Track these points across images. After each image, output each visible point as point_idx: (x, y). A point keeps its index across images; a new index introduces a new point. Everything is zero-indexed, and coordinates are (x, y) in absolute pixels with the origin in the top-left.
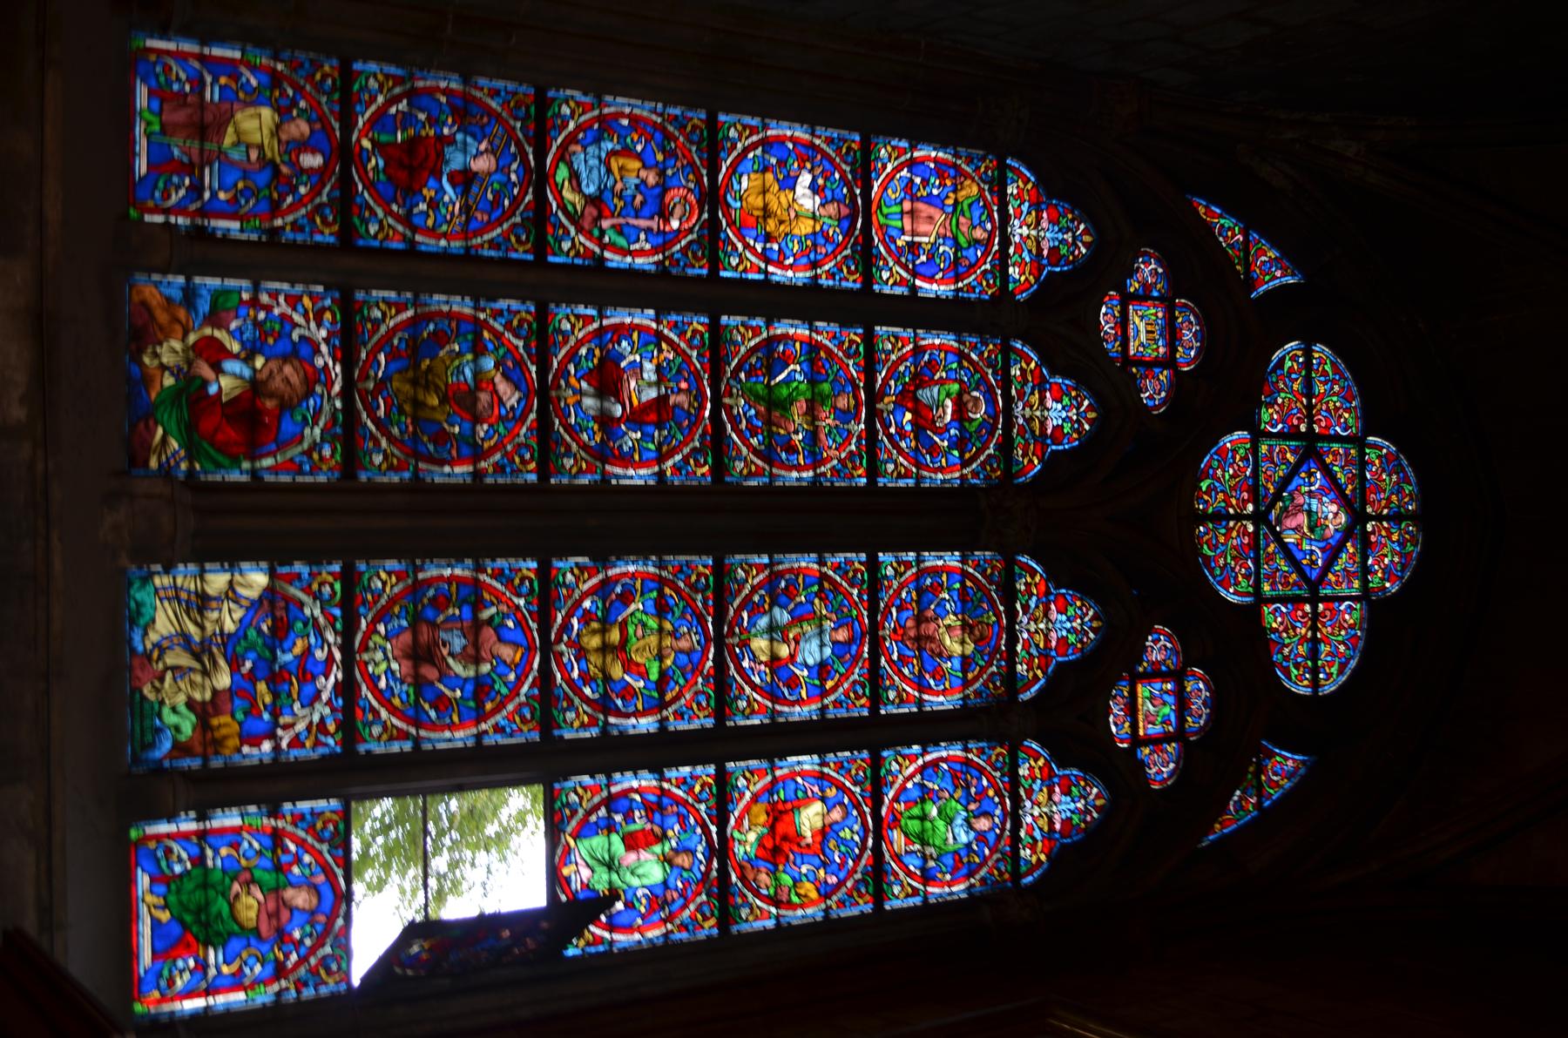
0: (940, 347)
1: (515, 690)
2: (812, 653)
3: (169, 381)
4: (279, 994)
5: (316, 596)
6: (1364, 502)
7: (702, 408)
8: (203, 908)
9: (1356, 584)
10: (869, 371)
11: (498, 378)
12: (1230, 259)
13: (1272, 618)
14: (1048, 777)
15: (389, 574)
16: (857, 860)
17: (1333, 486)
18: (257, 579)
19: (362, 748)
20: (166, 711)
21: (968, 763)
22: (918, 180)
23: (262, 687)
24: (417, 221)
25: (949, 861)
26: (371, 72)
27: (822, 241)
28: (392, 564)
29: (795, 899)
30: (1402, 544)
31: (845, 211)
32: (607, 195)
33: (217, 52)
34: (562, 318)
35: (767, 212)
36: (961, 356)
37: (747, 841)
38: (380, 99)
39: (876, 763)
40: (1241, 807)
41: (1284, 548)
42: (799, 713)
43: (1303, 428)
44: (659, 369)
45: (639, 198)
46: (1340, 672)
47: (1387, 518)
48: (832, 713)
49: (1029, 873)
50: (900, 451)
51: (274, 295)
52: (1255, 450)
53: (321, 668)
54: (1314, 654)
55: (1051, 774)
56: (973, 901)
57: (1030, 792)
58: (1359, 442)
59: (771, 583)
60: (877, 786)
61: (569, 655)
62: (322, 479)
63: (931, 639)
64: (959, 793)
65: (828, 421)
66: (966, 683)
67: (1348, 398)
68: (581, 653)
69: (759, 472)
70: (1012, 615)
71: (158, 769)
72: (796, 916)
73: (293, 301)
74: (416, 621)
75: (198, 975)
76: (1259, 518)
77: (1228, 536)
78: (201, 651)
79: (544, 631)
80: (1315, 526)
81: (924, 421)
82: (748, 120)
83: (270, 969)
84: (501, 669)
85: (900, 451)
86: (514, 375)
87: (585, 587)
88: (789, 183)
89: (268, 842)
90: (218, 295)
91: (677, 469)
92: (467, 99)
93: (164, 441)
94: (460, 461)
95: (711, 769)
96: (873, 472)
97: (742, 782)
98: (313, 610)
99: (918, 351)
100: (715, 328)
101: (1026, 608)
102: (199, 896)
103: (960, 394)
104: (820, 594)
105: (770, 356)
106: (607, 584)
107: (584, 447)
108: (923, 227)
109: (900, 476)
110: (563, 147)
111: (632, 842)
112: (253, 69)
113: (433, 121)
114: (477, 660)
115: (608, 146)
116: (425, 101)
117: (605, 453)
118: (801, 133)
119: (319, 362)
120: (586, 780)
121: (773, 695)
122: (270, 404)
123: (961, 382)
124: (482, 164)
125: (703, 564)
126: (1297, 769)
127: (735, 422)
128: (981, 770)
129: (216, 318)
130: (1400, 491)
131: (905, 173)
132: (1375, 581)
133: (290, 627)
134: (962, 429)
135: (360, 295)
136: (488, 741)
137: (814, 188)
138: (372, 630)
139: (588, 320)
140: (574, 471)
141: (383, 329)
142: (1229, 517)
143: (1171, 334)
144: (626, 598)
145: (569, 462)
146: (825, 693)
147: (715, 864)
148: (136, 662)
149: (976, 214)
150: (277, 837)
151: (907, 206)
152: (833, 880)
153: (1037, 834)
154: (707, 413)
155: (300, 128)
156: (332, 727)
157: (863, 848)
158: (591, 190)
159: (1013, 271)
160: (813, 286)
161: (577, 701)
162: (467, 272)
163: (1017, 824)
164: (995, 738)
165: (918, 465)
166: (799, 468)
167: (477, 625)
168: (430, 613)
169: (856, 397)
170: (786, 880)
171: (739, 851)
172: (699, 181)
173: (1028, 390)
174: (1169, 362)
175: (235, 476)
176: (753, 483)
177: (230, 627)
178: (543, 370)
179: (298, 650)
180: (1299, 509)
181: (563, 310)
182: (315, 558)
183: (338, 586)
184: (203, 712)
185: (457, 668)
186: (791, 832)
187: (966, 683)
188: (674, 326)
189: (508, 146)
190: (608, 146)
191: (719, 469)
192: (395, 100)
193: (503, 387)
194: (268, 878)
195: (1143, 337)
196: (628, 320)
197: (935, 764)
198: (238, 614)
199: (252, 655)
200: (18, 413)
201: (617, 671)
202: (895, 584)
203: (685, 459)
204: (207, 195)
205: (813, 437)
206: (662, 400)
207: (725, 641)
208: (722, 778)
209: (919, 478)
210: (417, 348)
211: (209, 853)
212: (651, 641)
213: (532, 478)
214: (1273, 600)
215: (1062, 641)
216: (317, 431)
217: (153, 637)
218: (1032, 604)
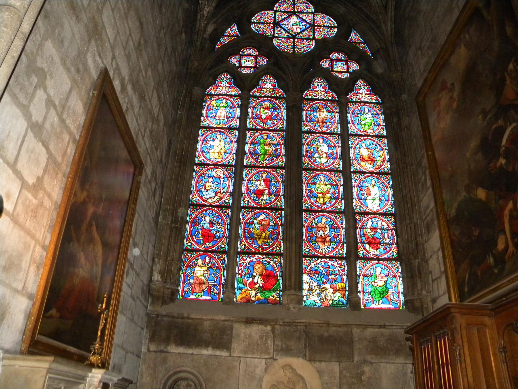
1: (333, 219)
2: (324, 148)
3: (259, 294)
4: (399, 277)
6: (290, 12)
7: (266, 171)
9: (310, 15)
10: (258, 130)
11: (259, 219)
12: (230, 41)
13: (319, 37)
14: (356, 94)
15: (305, 247)
18: (305, 278)
19: (345, 256)
20: (335, 299)
21: (352, 113)
22: (211, 115)
23: (330, 277)
24: (221, 236)
25: (375, 119)
26: (187, 244)
27: (226, 140)
29: (383, 157)
30: (301, 3)
31: (219, 133)
32: (215, 190)
33: (182, 280)
34: (244, 203)
36: (254, 107)
37: (369, 167)
38: (193, 243)
39: (352, 135)
40: (364, 47)
41: (301, 32)
42: (340, 153)
43: (272, 25)
44: (256, 181)
45: (216, 183)
46: (332, 21)
47: (294, 6)
48: (340, 145)
49: (378, 100)
50: (277, 124)
53: (327, 264)
56: (385, 114)
57: (359, 99)
60: (356, 135)
62: (282, 261)
63: (322, 120)
64: (359, 115)
65: (269, 141)
66: (333, 112)
69: (282, 158)
71: (349, 301)
72: (387, 157)
73: (240, 265)
74: (316, 241)
75: (395, 294)
76: (294, 38)
78: (322, 291)
81: (270, 118)
82: (197, 156)
83: (394, 279)
84: (328, 222)
85: (277, 124)
87: (309, 202)
88: (212, 147)
89: (366, 278)
90: (239, 282)
92: (192, 222)
93: (273, 296)
94: (278, 229)
95: (352, 174)
96: (282, 131)
97: (355, 167)
98: (312, 265)
99: (253, 118)
100: (247, 167)
101: (315, 96)
102: (377, 294)
103: (263, 108)
106: (308, 196)
107: (275, 200)
108: (222, 115)
109: (283, 124)
110: (204, 200)
111: (369, 195)
112: (186, 271)
113: (198, 231)
114: (326, 228)
115: (203, 190)
116: (193, 232)
117: (277, 195)
118: (199, 143)
119: (255, 260)
120: (354, 204)
122: (264, 272)
123: (260, 108)
124: (208, 219)
126: (355, 34)
127: (269, 163)
128: (354, 110)
131: (209, 118)
132: (309, 11)
133: (317, 270)
134: (272, 108)
135: (239, 250)
136: (344, 226)
137: (214, 140)
138: (318, 252)
139: (245, 197)
140: (281, 202)
141: (247, 245)
142: (294, 45)
143: (249, 56)
144: (312, 192)
145: (279, 204)
146: (335, 146)
147: (374, 175)
148: (324, 305)
149: (219, 101)
150: (364, 276)
151: (217, 118)
152: (379, 148)
153: (370, 97)
154: (268, 170)
155: (200, 262)
156: (340, 262)
157: (372, 140)
158: (213, 194)
159: (233, 93)
160: (238, 142)
161: (336, 205)
162: (234, 224)
163: (367, 102)
165: (281, 120)
166: (281, 149)
167: (317, 227)
168: (314, 238)
169: (264, 134)
170: (379, 159)
171: (372, 169)
172: (212, 168)
173: (262, 92)
175: (281, 281)
176: (284, 160)
177: (316, 284)
179: (322, 269)
180: (292, 28)
181: (242, 202)
183: (307, 259)
184: (335, 290)
185: (327, 233)
186: (367, 156)
189: (203, 213)
190: (203, 190)
191: (281, 168)
192: (193, 239)
193: (262, 217)
195: (250, 63)
196: (245, 188)
197: (352, 121)
198: (314, 282)
199: (323, 279)
200: (269, 328)
201: (329, 195)
202: (309, 127)
203: (279, 176)
204: (215, 284)
205: (273, 144)
206: (264, 180)
207: (322, 169)
208: (354, 172)
211: (367, 291)
213: (283, 212)
214: (314, 36)
216: (271, 262)
217: (318, 301)
218: (314, 94)
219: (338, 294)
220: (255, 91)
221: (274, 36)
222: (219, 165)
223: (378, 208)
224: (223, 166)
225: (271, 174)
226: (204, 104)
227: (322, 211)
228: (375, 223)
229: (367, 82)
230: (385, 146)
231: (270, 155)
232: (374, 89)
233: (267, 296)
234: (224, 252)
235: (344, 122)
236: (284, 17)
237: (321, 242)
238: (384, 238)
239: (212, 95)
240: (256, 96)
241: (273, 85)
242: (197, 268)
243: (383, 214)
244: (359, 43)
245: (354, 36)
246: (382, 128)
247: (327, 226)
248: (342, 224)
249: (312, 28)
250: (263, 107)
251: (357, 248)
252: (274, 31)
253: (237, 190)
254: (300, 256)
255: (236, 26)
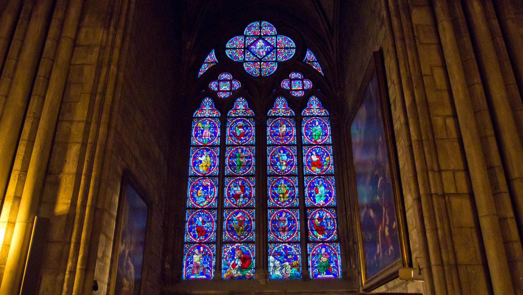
0: (229, 131)
2: (285, 158)
3: (239, 272)
5: (274, 248)
6: (257, 36)
8: (324, 267)
9: (274, 38)
16: (322, 149)
17: (254, 44)
18: (271, 258)
21: (306, 126)
23: (289, 257)
28: (269, 235)
31: (205, 150)
33: (185, 265)
35: (206, 166)
39: (305, 145)
40: (317, 66)
42: (296, 160)
43: (243, 50)
44: (235, 187)
51: (224, 255)
52: (247, 62)
54: (287, 48)
55: (309, 108)
57: (312, 113)
58: (245, 36)
59: (273, 166)
61: (285, 204)
63: (283, 134)
67: (236, 39)
68: (284, 202)
69: (253, 168)
70: (279, 116)
71: (302, 274)
72: (332, 161)
73: (225, 252)
76: (260, 61)
77: (264, 68)
78: (282, 267)
79: (280, 208)
80: (261, 46)
81: (243, 135)
86: (237, 213)
88: (201, 162)
90: (225, 264)
91: (253, 184)
94: (251, 223)
96: (252, 145)
98: (276, 249)
99: (230, 136)
101: (277, 113)
102: (322, 268)
104: (274, 156)
105: (232, 165)
107: (249, 201)
108: (207, 134)
110: (197, 205)
113: (194, 228)
114: (285, 220)
117: (250, 198)
118: (191, 159)
120: (306, 201)
121: (292, 166)
122: (242, 256)
125: (269, 179)
127: (244, 172)
128: (307, 123)
129: (229, 265)
130: (255, 27)
132: (273, 33)
137: (201, 157)
140: (253, 203)
143: (225, 80)
150: (313, 255)
151: (203, 138)
155: (196, 251)
163: (318, 116)
164: (302, 120)
166: (252, 160)
167: (279, 220)
171: (319, 172)
172: (201, 179)
174: (231, 81)
175: (254, 262)
177: (279, 262)
178: (235, 208)
180: (259, 52)
181: (225, 204)
182: (267, 248)
184: (292, 267)
185: (286, 224)
187: (291, 126)
188: (227, 184)
191: (252, 176)
193: (239, 215)
194: (319, 256)
195: (226, 87)
201: (287, 195)
206: (240, 186)
208: (307, 175)
209: (253, 136)
210: (232, 230)
212: (282, 189)
213: (254, 210)
215: (284, 106)
219: (294, 269)
220: (231, 113)
221: (244, 61)
222: (207, 176)
223: (324, 203)
224: (209, 176)
225: (245, 181)
226: (193, 126)
227: (283, 208)
228: (321, 214)
229: (318, 98)
230: (330, 152)
231: (244, 166)
232: (324, 104)
233: (244, 273)
234: (213, 243)
235: (299, 135)
236: (252, 41)
237: (282, 231)
238: (327, 225)
239: (198, 117)
240: (232, 117)
241: (245, 106)
242: (195, 256)
243: (328, 208)
244: (312, 62)
245: (310, 56)
246: (329, 137)
247: (286, 219)
248: (297, 217)
249: (275, 50)
250: (237, 126)
251: (307, 234)
252: (244, 56)
253: (220, 195)
254: (266, 242)
255: (214, 53)
